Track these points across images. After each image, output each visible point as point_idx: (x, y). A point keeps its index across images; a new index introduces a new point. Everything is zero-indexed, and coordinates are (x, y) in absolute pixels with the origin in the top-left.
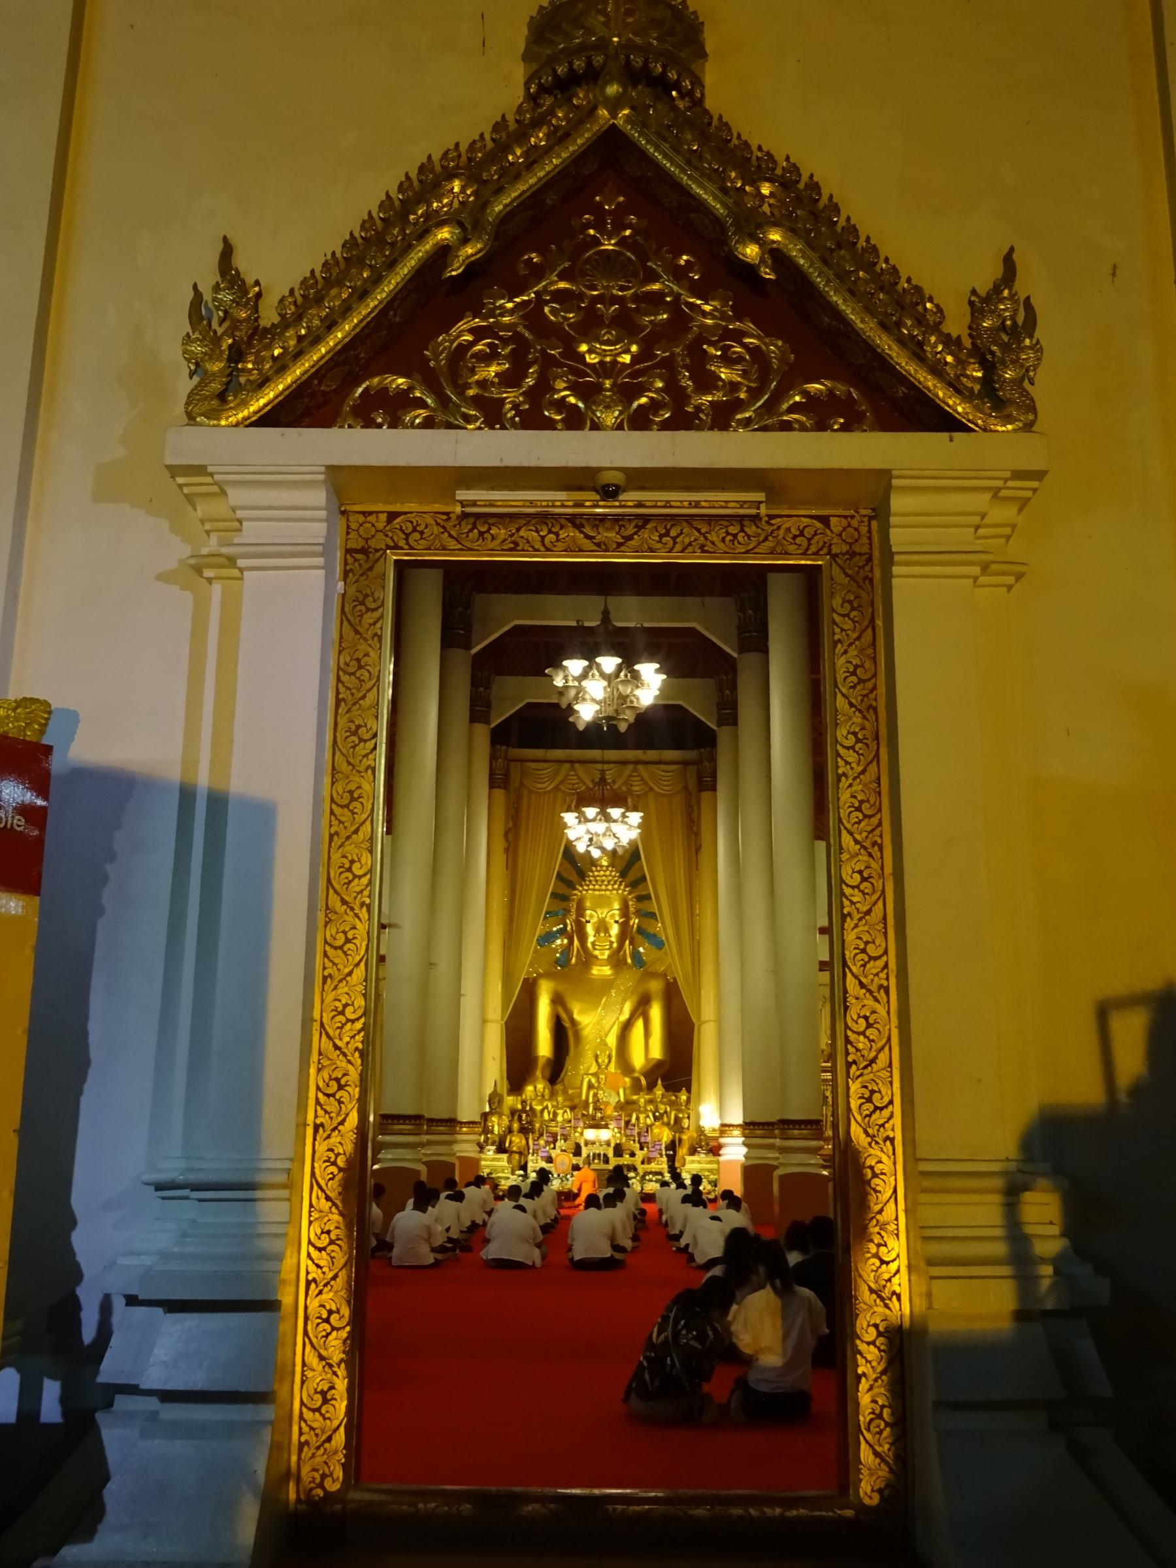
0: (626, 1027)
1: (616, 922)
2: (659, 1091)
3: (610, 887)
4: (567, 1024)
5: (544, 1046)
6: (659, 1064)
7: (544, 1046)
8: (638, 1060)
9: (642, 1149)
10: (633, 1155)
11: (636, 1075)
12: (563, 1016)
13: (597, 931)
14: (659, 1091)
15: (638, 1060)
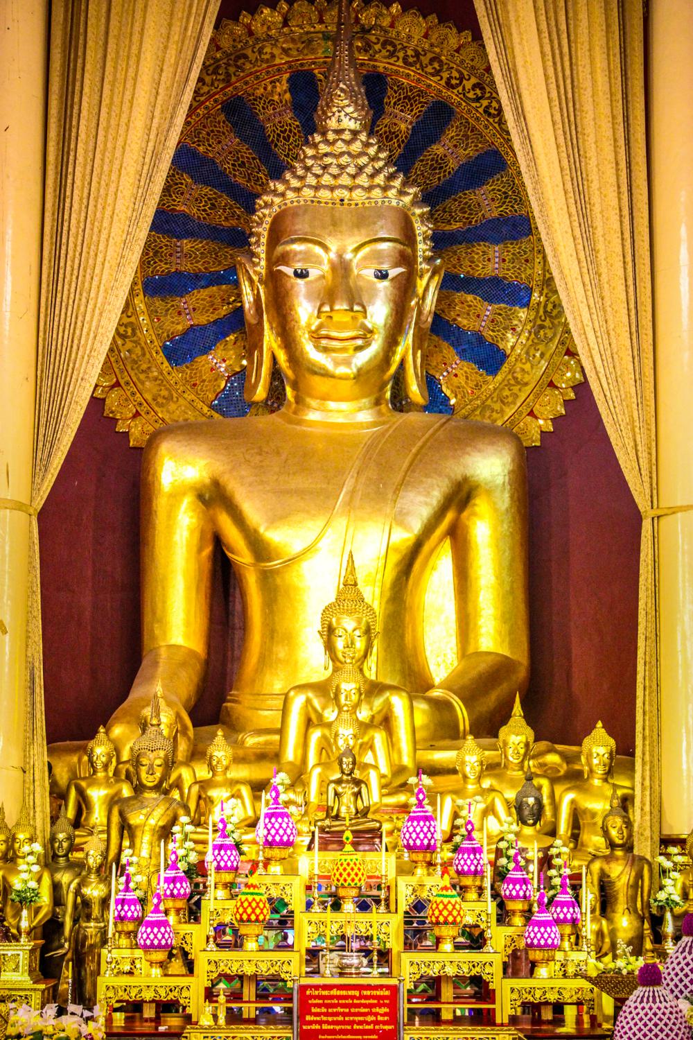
0: (409, 563)
1: (382, 276)
2: (516, 735)
3: (363, 180)
4: (242, 555)
5: (178, 619)
6: (499, 670)
7: (178, 619)
8: (441, 659)
9: (503, 917)
10: (475, 940)
11: (436, 693)
12: (233, 535)
13: (328, 296)
14: (516, 735)
15: (441, 659)
